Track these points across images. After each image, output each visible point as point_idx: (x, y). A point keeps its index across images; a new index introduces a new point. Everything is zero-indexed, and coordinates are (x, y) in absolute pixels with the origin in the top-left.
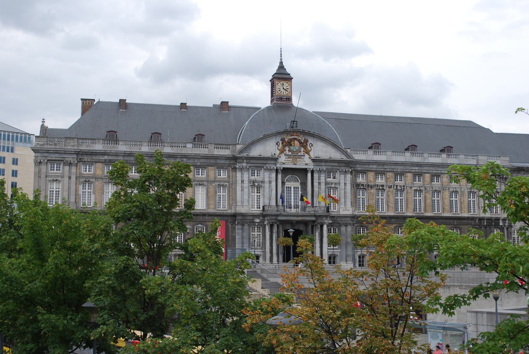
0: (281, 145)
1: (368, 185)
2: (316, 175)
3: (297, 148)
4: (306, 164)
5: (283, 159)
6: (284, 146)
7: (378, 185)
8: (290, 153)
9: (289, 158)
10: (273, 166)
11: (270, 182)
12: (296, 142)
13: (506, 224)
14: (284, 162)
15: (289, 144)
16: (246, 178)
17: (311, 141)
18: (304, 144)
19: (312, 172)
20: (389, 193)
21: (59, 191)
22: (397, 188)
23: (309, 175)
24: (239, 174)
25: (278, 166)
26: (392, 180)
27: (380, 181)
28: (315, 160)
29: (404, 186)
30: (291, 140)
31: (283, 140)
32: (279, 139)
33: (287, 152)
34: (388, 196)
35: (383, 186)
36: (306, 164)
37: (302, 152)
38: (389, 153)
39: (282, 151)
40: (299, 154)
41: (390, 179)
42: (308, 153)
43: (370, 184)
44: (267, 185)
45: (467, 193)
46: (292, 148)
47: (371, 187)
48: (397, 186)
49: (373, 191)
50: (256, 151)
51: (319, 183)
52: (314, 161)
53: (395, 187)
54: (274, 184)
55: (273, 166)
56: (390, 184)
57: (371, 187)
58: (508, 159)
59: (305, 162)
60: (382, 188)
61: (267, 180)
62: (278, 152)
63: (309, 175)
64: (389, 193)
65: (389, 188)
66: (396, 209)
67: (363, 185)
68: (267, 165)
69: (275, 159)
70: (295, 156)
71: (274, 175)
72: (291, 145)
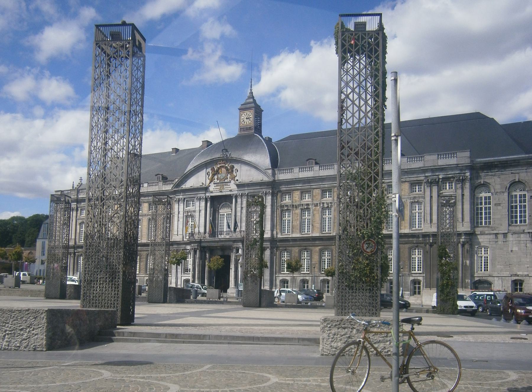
0: (211, 175)
1: (293, 205)
2: (239, 200)
3: (224, 175)
4: (231, 191)
5: (211, 188)
6: (214, 175)
7: (302, 205)
8: (218, 182)
9: (217, 186)
10: (203, 195)
11: (200, 211)
12: (224, 170)
13: (461, 240)
14: (214, 190)
16: (181, 210)
17: (236, 166)
18: (230, 171)
19: (236, 197)
20: (315, 212)
21: (487, 257)
22: (323, 205)
23: (234, 200)
24: (176, 206)
25: (207, 194)
26: (319, 197)
27: (307, 199)
28: (239, 186)
29: (331, 203)
30: (219, 169)
31: (213, 169)
32: (209, 170)
33: (216, 180)
34: (314, 215)
35: (308, 205)
37: (229, 179)
38: (316, 168)
40: (226, 181)
41: (317, 197)
42: (233, 178)
43: (294, 204)
44: (197, 214)
45: (409, 204)
46: (219, 176)
47: (296, 207)
48: (323, 203)
49: (298, 211)
50: (191, 183)
51: (242, 208)
52: (239, 186)
53: (322, 205)
54: (203, 212)
55: (203, 195)
56: (315, 202)
57: (296, 207)
58: (467, 154)
59: (231, 188)
60: (306, 208)
61: (197, 209)
62: (208, 181)
63: (234, 200)
64: (315, 212)
65: (315, 206)
66: (322, 229)
67: (287, 206)
68: (199, 195)
69: (206, 189)
70: (223, 183)
71: (203, 204)
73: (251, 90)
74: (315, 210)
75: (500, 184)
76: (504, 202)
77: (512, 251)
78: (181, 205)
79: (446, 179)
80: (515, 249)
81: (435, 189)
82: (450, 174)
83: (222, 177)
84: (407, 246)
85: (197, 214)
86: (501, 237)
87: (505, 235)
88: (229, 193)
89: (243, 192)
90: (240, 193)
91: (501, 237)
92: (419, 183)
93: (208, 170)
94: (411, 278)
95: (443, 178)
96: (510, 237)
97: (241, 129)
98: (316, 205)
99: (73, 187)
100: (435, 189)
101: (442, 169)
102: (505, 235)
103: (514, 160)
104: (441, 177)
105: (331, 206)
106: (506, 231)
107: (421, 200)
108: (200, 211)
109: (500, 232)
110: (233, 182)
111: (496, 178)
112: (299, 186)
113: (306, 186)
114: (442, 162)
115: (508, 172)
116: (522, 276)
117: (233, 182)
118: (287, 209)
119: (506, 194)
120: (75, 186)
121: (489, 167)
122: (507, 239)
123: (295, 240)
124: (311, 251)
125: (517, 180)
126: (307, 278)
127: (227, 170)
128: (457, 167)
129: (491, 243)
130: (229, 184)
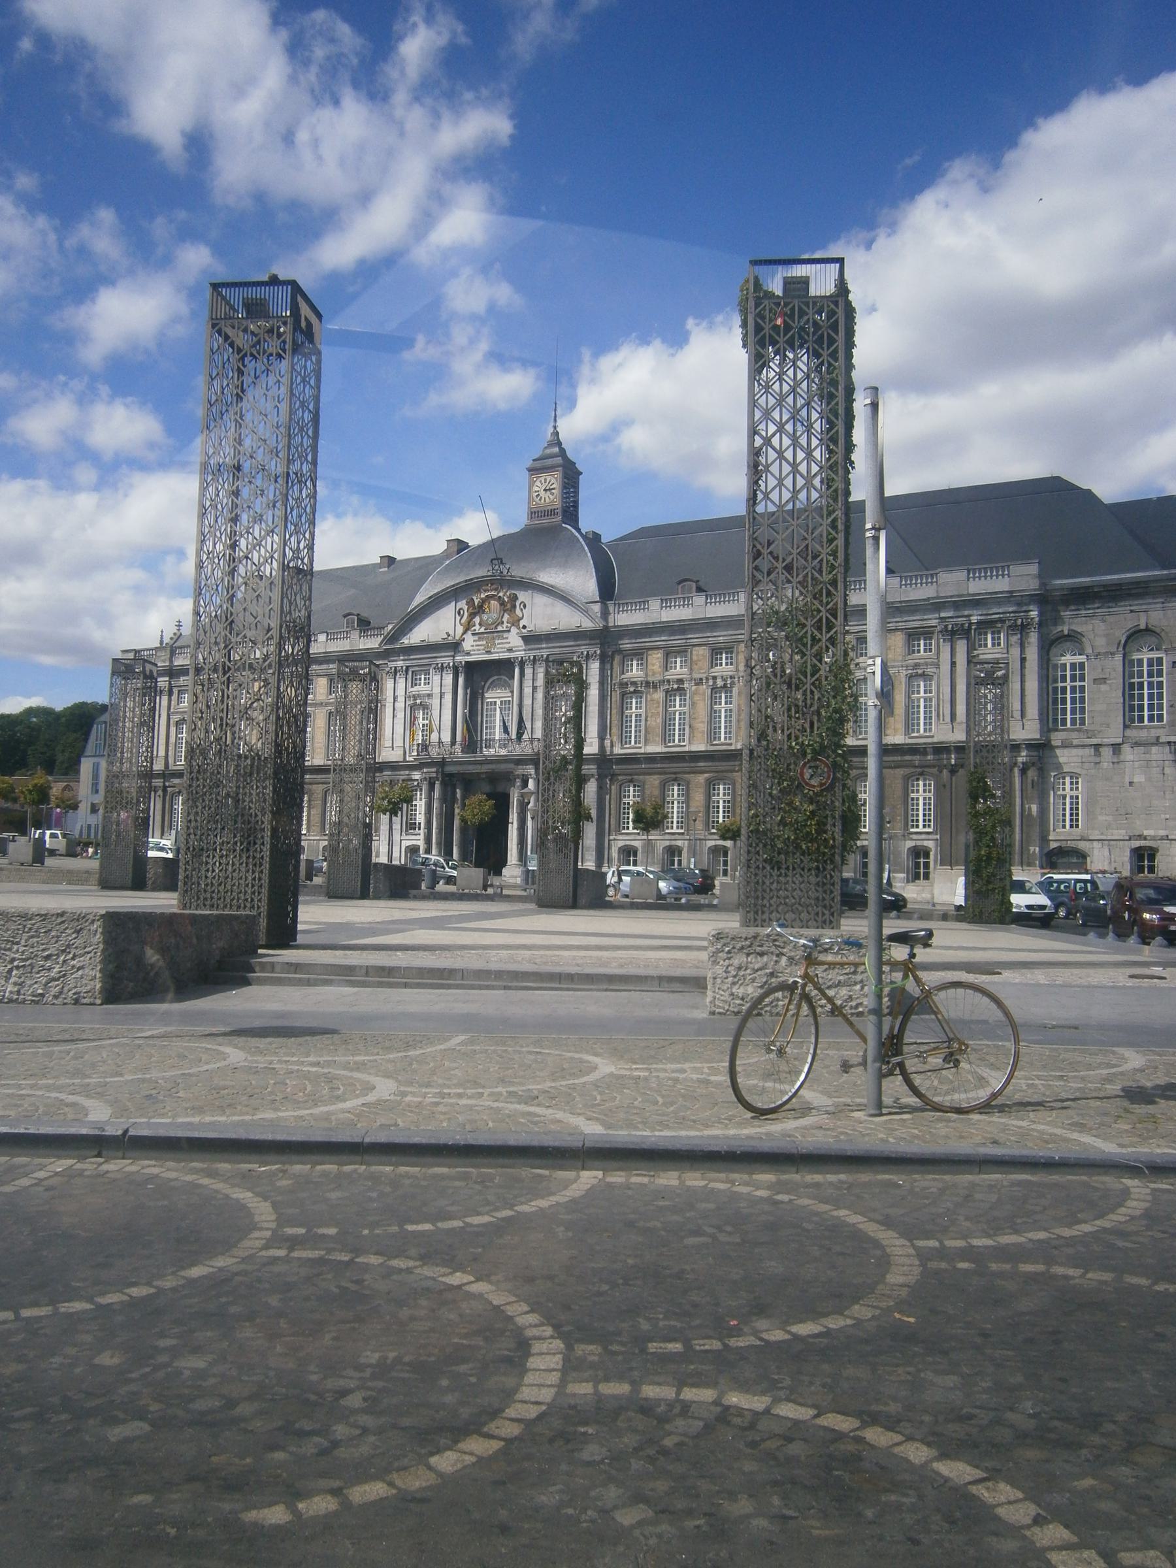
0: (466, 614)
1: (648, 683)
2: (528, 671)
3: (495, 616)
4: (510, 650)
5: (469, 643)
6: (472, 615)
7: (669, 681)
8: (482, 630)
9: (479, 639)
10: (449, 661)
11: (442, 695)
12: (494, 603)
13: (1020, 760)
14: (474, 649)
15: (477, 610)
16: (401, 692)
17: (522, 596)
18: (509, 606)
19: (522, 664)
20: (696, 698)
21: (1077, 797)
22: (715, 683)
23: (517, 671)
24: (389, 684)
25: (458, 658)
26: (706, 664)
28: (529, 639)
29: (731, 677)
30: (483, 601)
31: (470, 603)
32: (462, 604)
33: (477, 627)
35: (680, 681)
36: (510, 650)
37: (505, 624)
38: (700, 599)
39: (468, 627)
40: (500, 628)
41: (700, 664)
42: (516, 622)
43: (650, 679)
44: (435, 702)
45: (903, 680)
46: (485, 617)
47: (655, 687)
48: (715, 678)
49: (659, 695)
50: (420, 634)
51: (534, 688)
52: (529, 639)
53: (711, 683)
54: (448, 697)
55: (449, 661)
56: (696, 676)
57: (655, 687)
58: (1033, 569)
59: (512, 644)
60: (677, 689)
61: (436, 690)
62: (460, 630)
63: (517, 671)
64: (696, 698)
65: (696, 684)
66: (712, 734)
67: (634, 684)
68: (439, 661)
69: (455, 646)
70: (492, 633)
71: (448, 679)
72: (484, 612)
73: (555, 427)
74: (695, 693)
75: (1107, 635)
76: (1113, 675)
77: (1131, 783)
78: (401, 683)
79: (986, 625)
80: (1139, 778)
81: (961, 646)
82: (995, 612)
83: (490, 621)
84: (900, 772)
85: (435, 702)
86: (1106, 752)
87: (1116, 748)
88: (506, 655)
89: (537, 653)
90: (531, 655)
91: (1106, 752)
92: (927, 633)
93: (459, 605)
94: (910, 844)
95: (979, 623)
96: (1128, 753)
97: (533, 514)
98: (699, 682)
99: (161, 642)
100: (961, 646)
101: (977, 602)
102: (1116, 748)
103: (1137, 583)
104: (974, 619)
105: (733, 683)
106: (1119, 740)
107: (930, 670)
108: (442, 695)
109: (1106, 741)
110: (514, 630)
111: (1096, 622)
112: (661, 640)
113: (677, 641)
114: (978, 586)
115: (1123, 608)
116: (1154, 838)
117: (514, 630)
118: (635, 692)
119: (1119, 658)
120: (166, 640)
121: (1082, 597)
122: (1122, 758)
123: (651, 758)
124: (688, 784)
125: (1143, 627)
126: (679, 843)
127: (503, 604)
128: (1009, 597)
129: (1086, 766)
130: (505, 635)
